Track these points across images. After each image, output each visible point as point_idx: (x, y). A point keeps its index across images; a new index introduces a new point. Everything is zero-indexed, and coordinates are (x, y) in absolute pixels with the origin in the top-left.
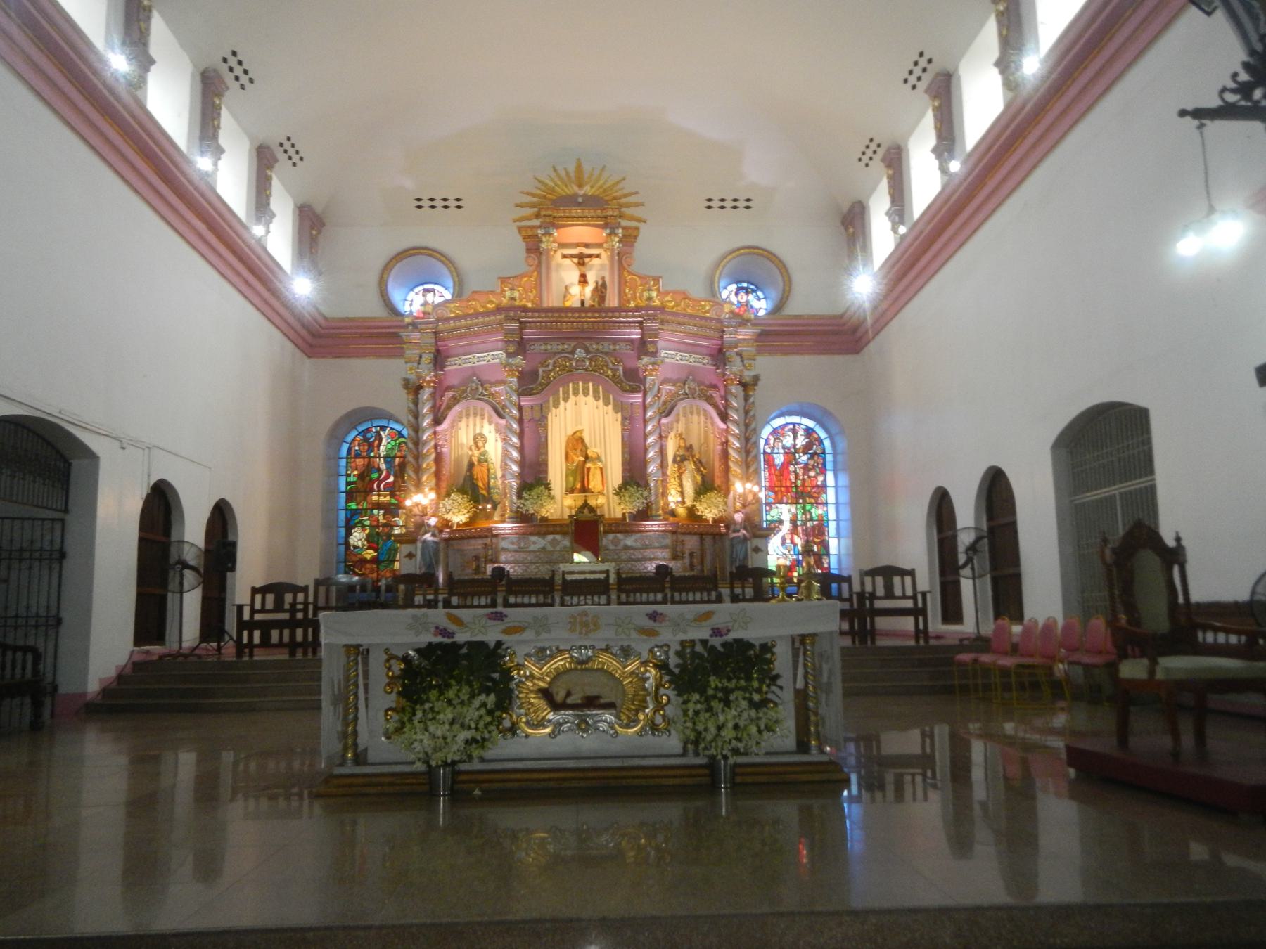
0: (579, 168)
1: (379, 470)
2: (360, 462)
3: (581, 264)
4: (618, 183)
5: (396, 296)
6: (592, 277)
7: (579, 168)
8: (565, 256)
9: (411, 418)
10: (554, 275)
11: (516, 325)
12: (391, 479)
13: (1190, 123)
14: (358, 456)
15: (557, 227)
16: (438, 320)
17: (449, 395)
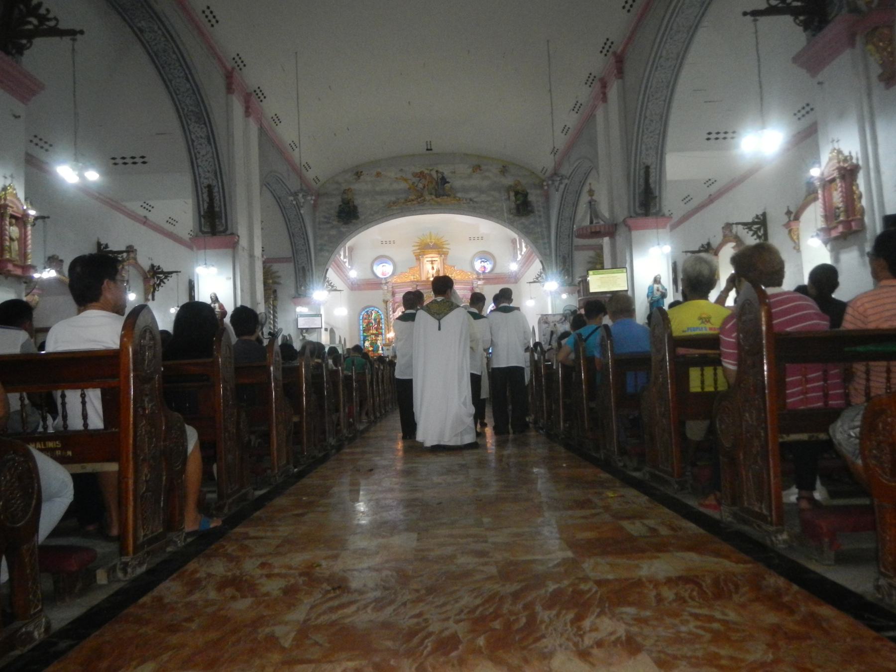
0: (430, 233)
1: (372, 323)
2: (366, 321)
3: (432, 263)
4: (442, 238)
5: (375, 268)
6: (435, 267)
7: (430, 233)
8: (427, 261)
9: (385, 310)
10: (424, 266)
11: (415, 286)
12: (376, 326)
13: (528, 284)
14: (365, 319)
15: (424, 255)
16: (393, 284)
17: (396, 304)
